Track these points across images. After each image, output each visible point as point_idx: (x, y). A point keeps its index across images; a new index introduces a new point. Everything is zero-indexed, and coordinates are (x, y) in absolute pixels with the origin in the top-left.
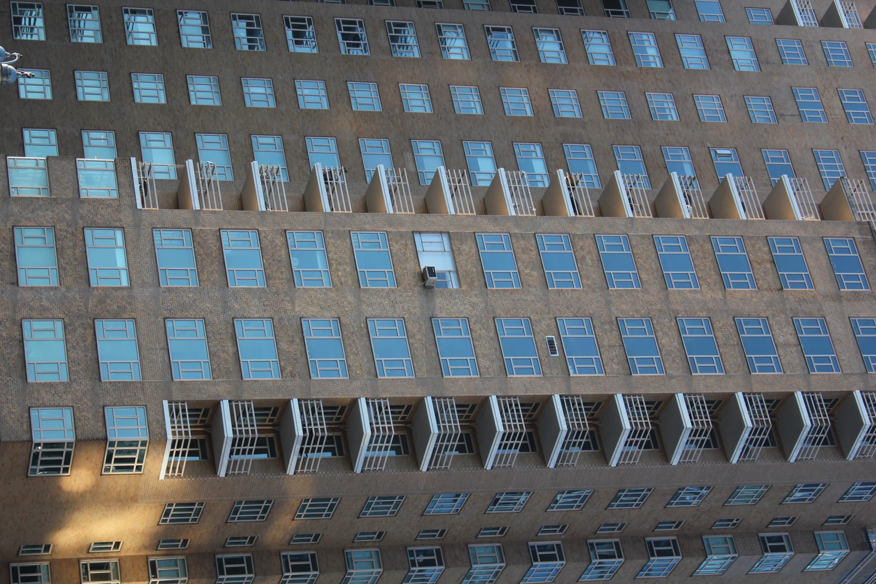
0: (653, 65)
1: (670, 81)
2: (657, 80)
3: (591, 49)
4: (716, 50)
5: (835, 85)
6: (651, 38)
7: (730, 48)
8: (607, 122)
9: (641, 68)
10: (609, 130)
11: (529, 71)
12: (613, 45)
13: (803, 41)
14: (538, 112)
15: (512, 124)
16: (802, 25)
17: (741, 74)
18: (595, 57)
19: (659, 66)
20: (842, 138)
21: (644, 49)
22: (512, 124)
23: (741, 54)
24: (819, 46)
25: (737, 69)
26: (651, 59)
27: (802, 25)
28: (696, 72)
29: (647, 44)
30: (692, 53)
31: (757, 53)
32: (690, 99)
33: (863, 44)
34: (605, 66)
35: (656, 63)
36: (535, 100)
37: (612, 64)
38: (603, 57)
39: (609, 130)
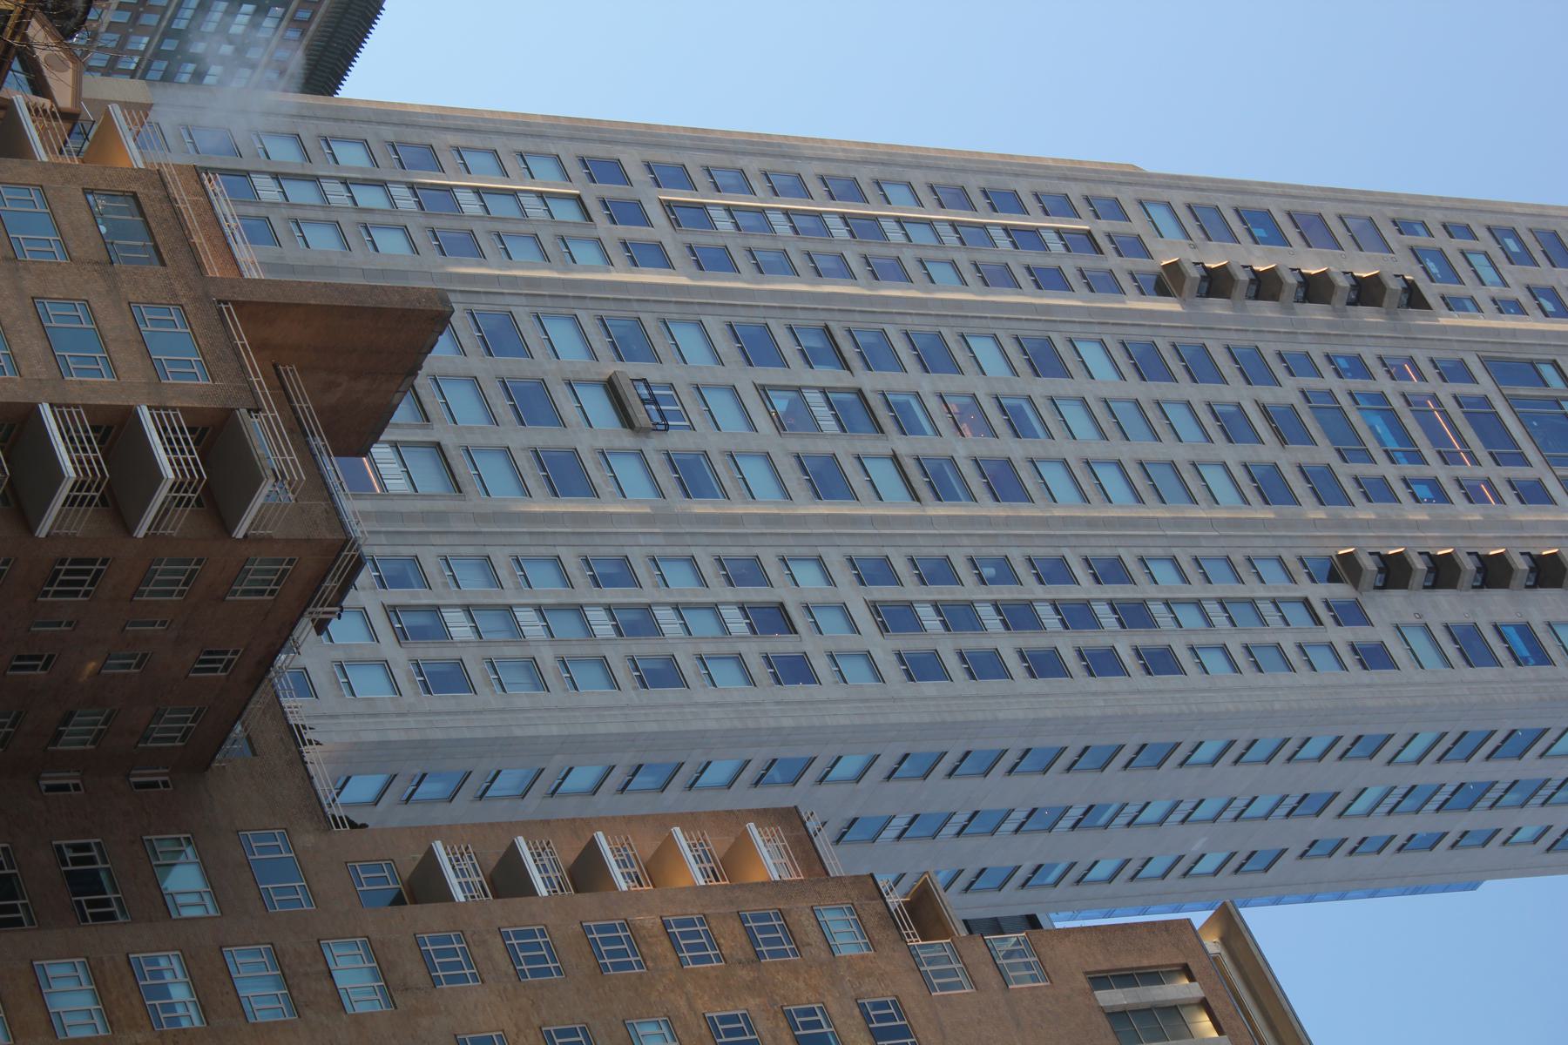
0: (185, 1024)
3: (57, 1004)
5: (536, 1021)
6: (175, 961)
7: (332, 966)
9: (161, 1035)
12: (101, 990)
13: (468, 934)
16: (462, 899)
17: (358, 1019)
18: (67, 1020)
19: (197, 1023)
21: (163, 991)
23: (353, 976)
24: (499, 939)
25: (350, 1011)
26: (180, 1010)
27: (462, 899)
28: (270, 1027)
29: (168, 977)
30: (258, 989)
31: (383, 972)
33: (577, 927)
34: (89, 1039)
35: (190, 1018)
37: (101, 1033)
38: (83, 1019)
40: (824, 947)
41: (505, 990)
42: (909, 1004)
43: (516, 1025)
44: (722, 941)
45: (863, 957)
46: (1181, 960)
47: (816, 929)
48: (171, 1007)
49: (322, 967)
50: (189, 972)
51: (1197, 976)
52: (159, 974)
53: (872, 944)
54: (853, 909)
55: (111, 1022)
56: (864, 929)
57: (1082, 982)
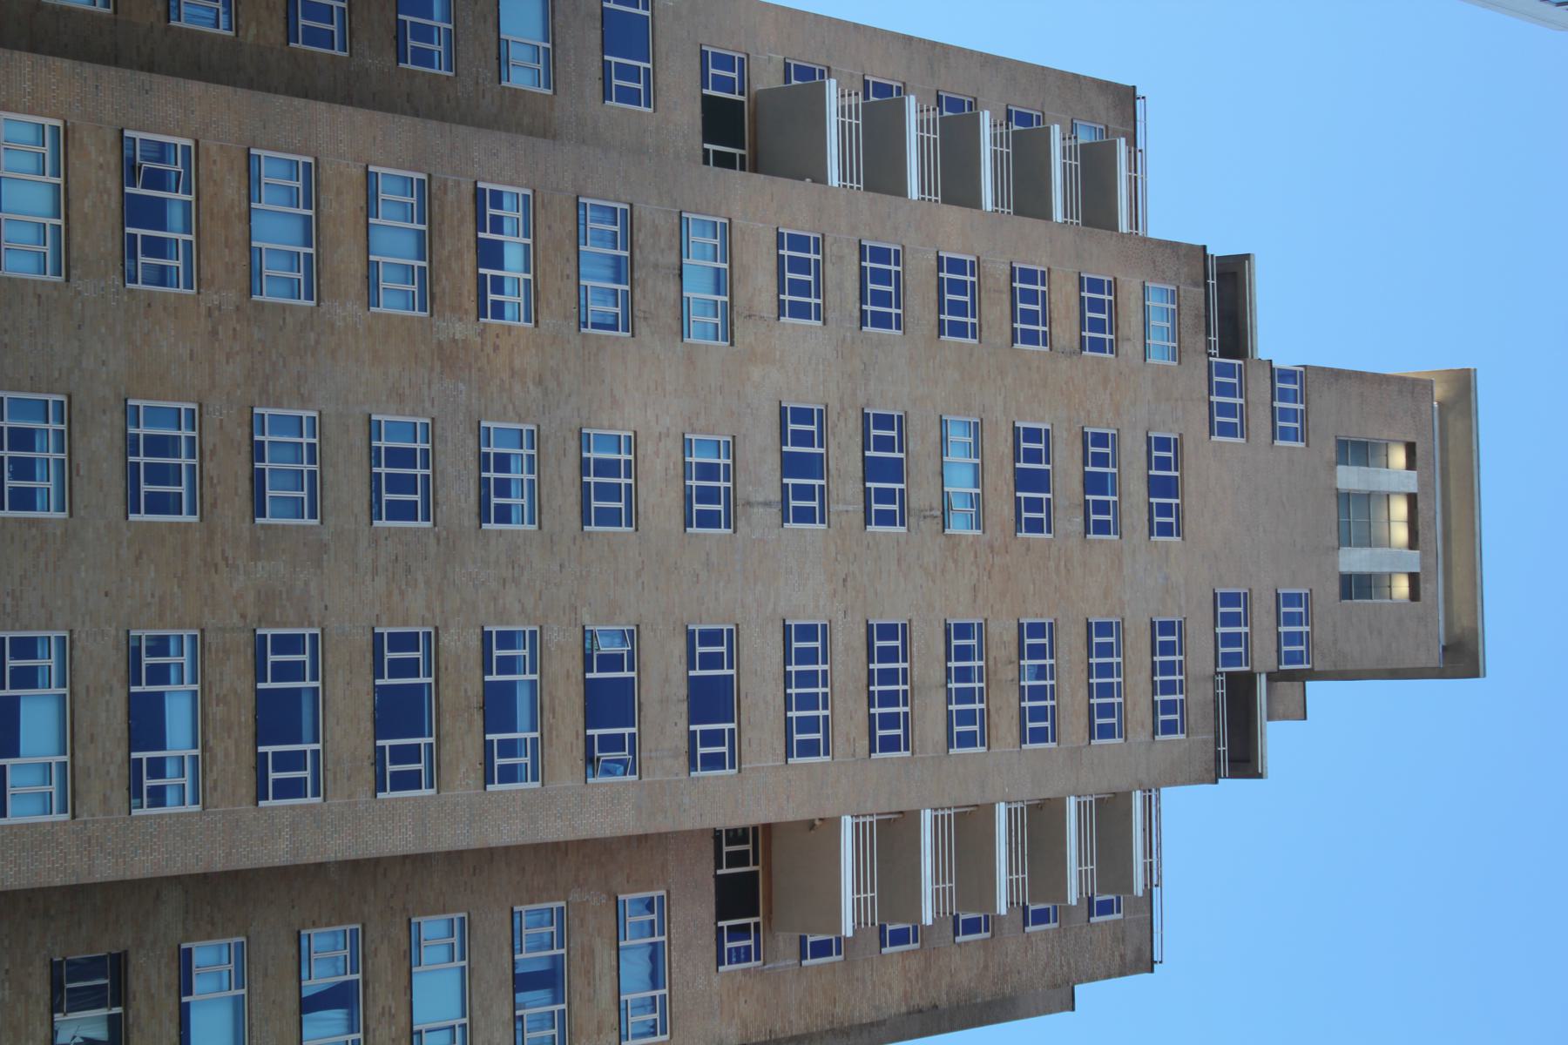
1: (540, 381)
2: (513, 373)
4: (656, 266)
7: (685, 260)
8: (376, 539)
10: (375, 572)
11: (214, 333)
13: (829, 240)
14: (214, 505)
15: (138, 558)
20: (845, 580)
22: (138, 558)
27: (836, 184)
32: (573, 445)
36: (213, 452)
39: (375, 572)
40: (1140, 348)
41: (844, 339)
42: (1189, 447)
43: (841, 400)
44: (1055, 315)
45: (1167, 369)
46: (1410, 439)
47: (1140, 316)
48: (498, 285)
49: (674, 259)
50: (530, 228)
51: (1419, 463)
52: (497, 224)
53: (1178, 354)
54: (1175, 296)
55: (428, 297)
56: (1177, 333)
57: (1330, 452)
